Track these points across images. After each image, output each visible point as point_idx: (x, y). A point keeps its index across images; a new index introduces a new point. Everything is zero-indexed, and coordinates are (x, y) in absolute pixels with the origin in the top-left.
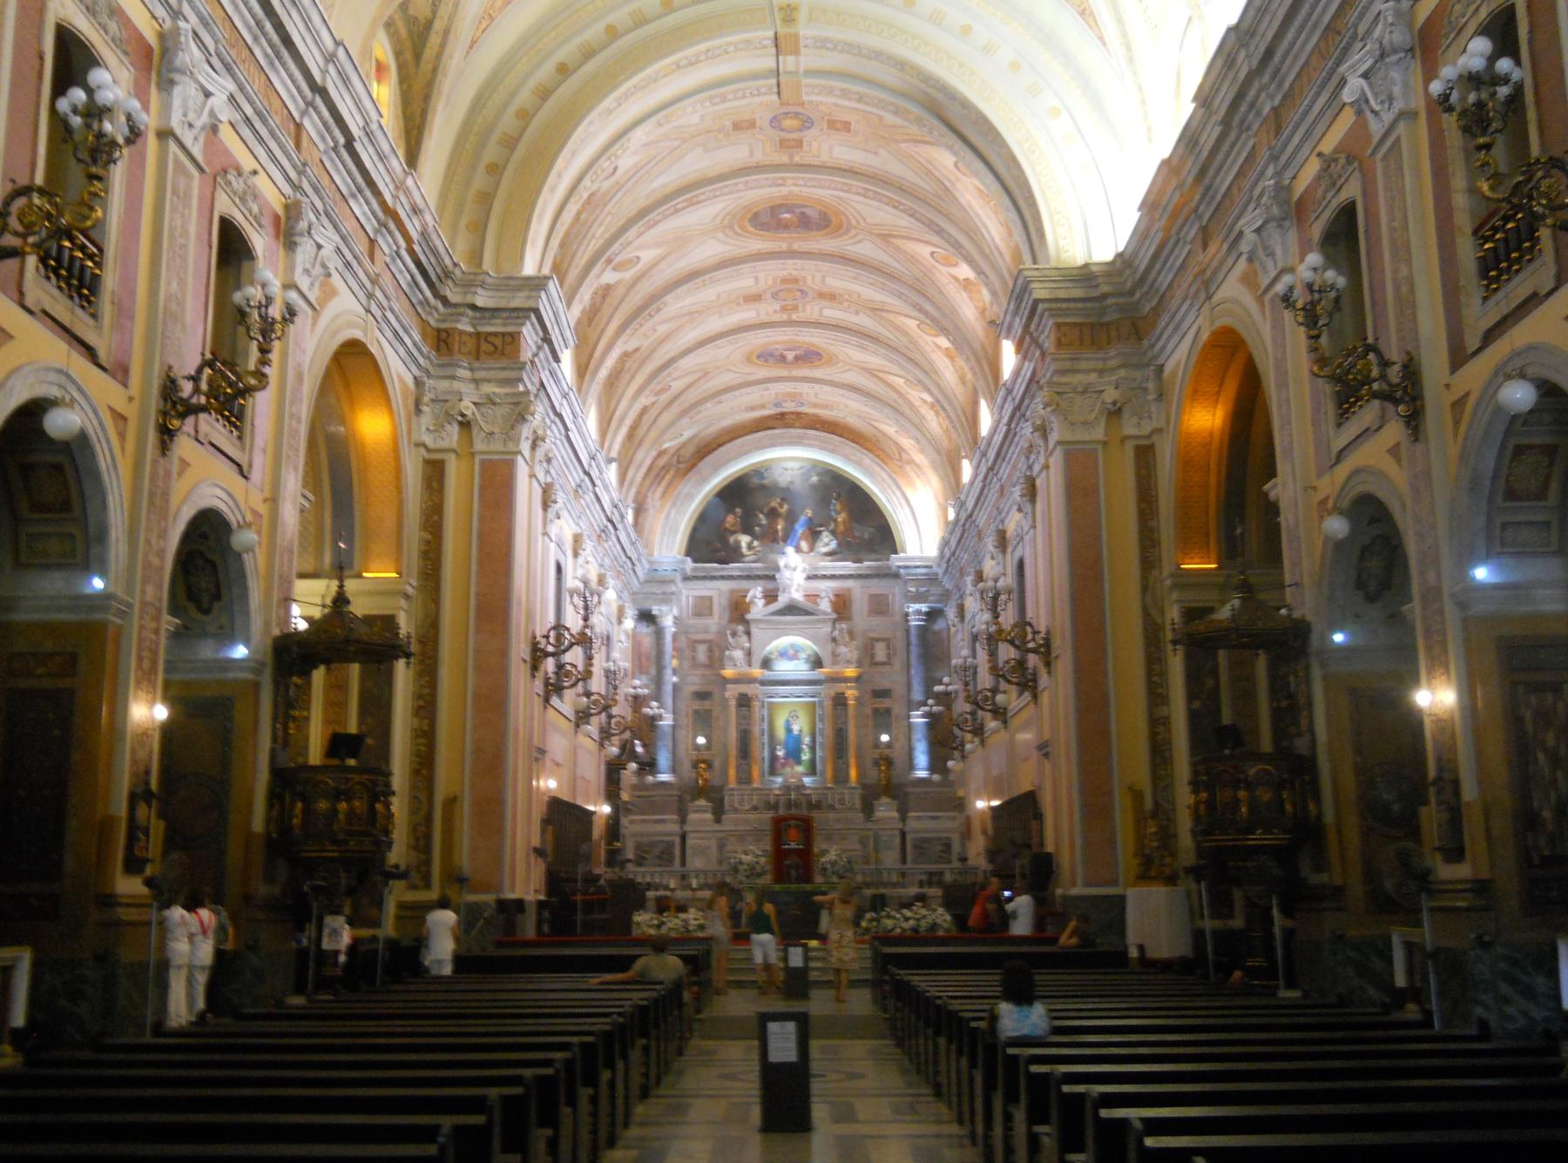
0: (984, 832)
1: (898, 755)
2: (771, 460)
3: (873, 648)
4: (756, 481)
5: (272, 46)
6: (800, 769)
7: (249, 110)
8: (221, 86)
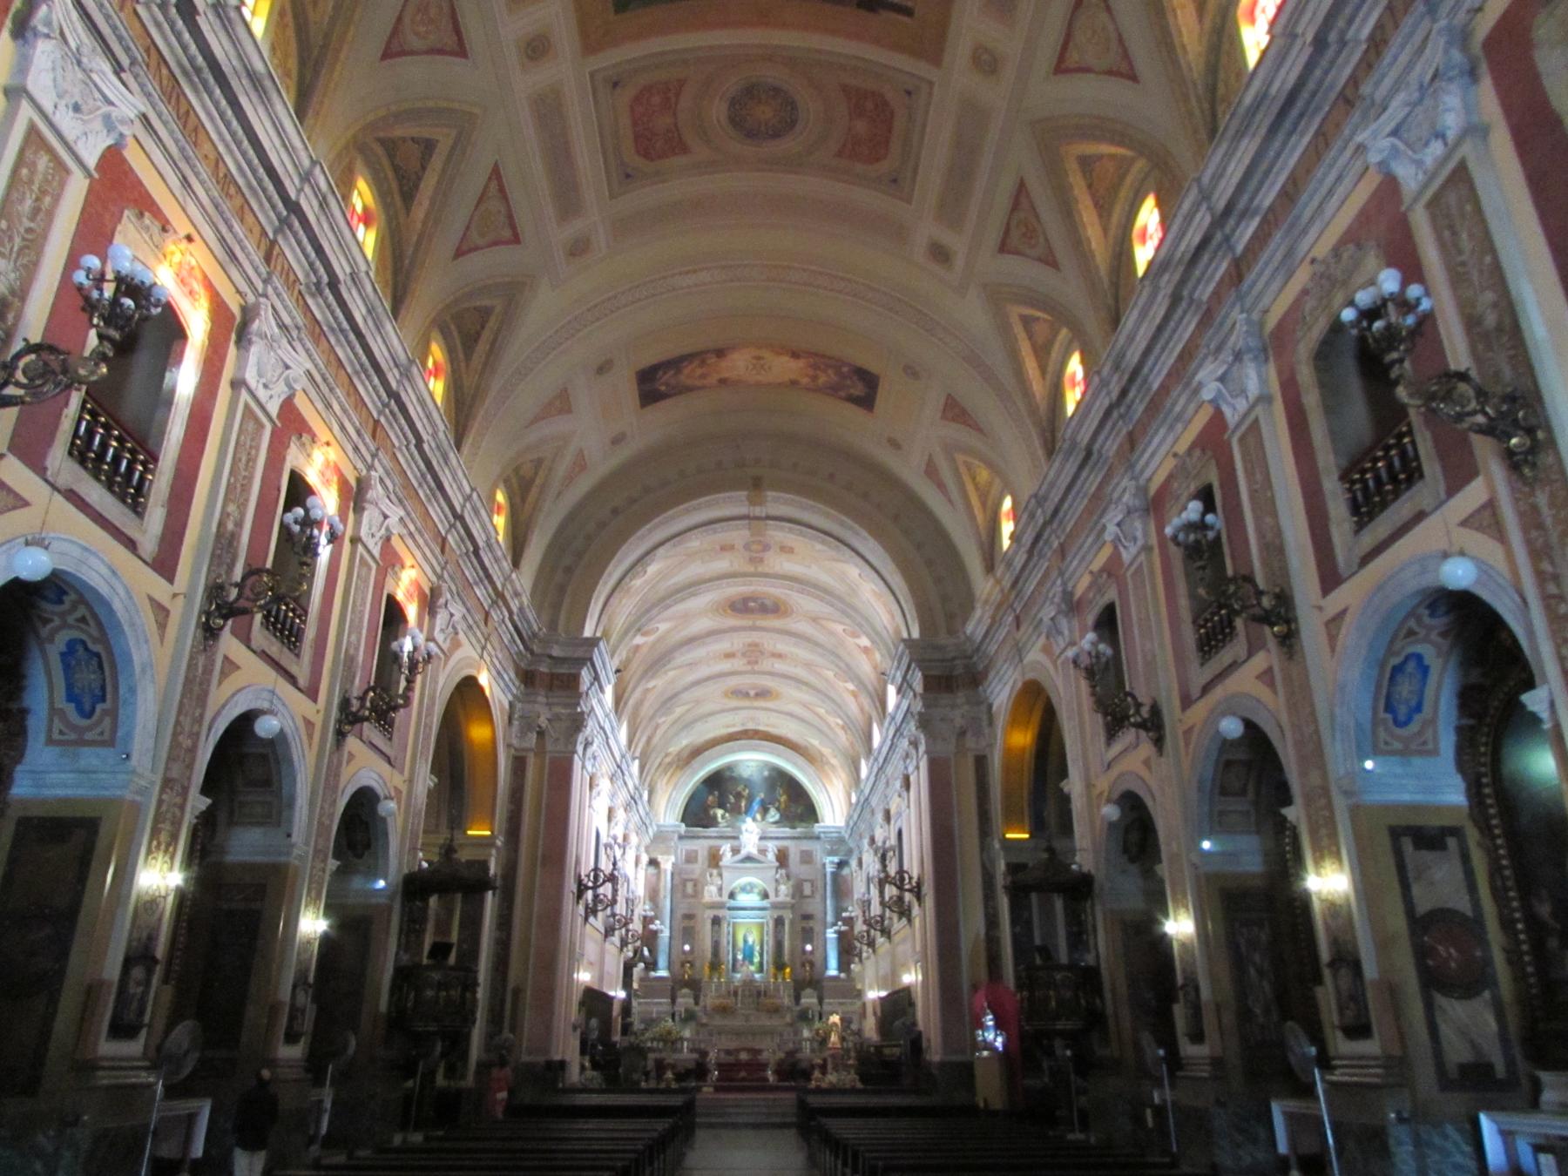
0: (875, 1014)
1: (817, 959)
2: (741, 761)
4: (728, 773)
5: (431, 490)
6: (752, 968)
7: (412, 528)
8: (395, 513)
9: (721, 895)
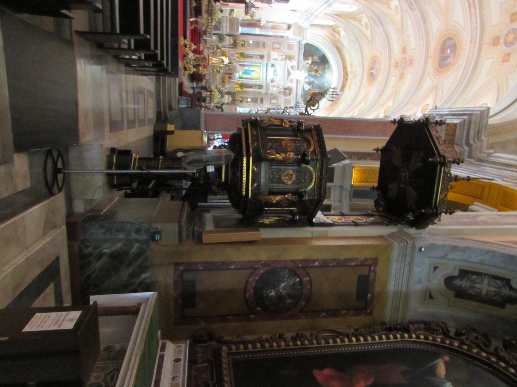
3: (276, 99)
4: (327, 66)
6: (241, 73)
9: (273, 60)
